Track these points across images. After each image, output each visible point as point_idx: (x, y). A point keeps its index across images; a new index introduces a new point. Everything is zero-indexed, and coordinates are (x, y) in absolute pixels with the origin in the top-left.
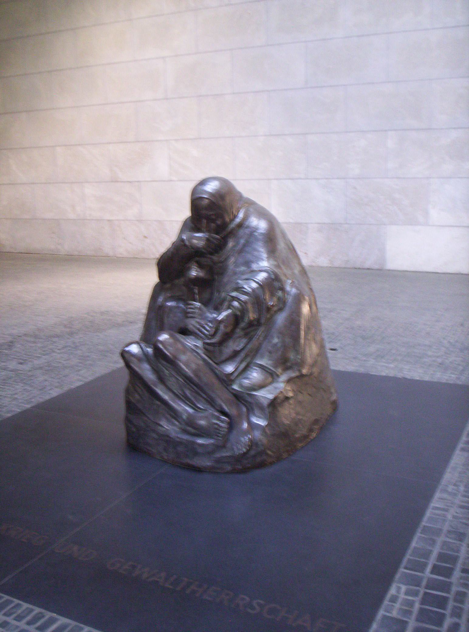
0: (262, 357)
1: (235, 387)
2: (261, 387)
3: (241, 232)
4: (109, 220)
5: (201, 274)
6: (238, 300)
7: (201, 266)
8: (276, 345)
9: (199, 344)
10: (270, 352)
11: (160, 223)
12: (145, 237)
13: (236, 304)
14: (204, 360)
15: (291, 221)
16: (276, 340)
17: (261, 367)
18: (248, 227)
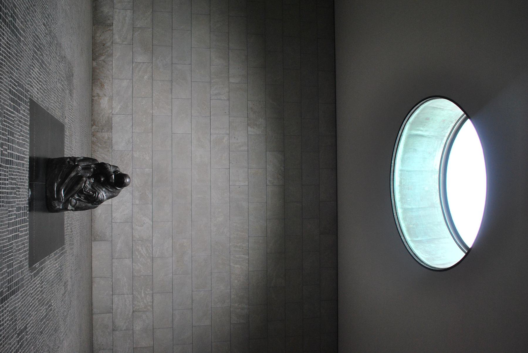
0: (79, 203)
1: (70, 198)
2: (71, 205)
3: (114, 189)
4: (113, 24)
5: (102, 181)
6: (95, 196)
7: (104, 180)
8: (82, 205)
9: (83, 187)
10: (81, 204)
11: (111, 55)
12: (104, 45)
13: (95, 195)
14: (78, 190)
15: (113, 124)
16: (84, 205)
17: (76, 203)
18: (116, 191)
